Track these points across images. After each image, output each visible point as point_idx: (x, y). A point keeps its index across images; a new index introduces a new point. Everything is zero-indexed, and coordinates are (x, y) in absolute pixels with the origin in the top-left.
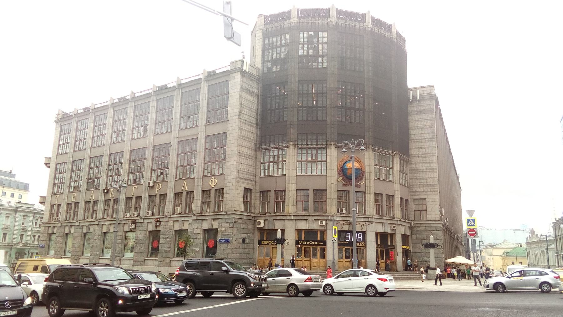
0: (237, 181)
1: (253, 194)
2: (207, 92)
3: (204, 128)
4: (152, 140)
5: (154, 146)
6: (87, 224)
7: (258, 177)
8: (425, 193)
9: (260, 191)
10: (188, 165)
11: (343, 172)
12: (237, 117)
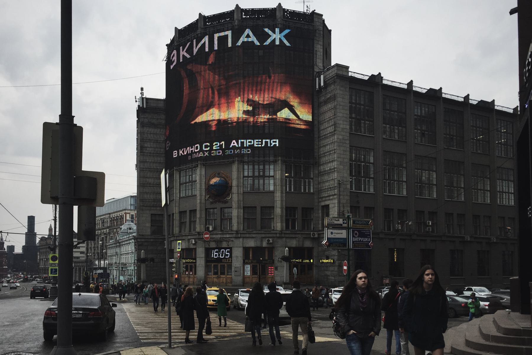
11: (209, 189)
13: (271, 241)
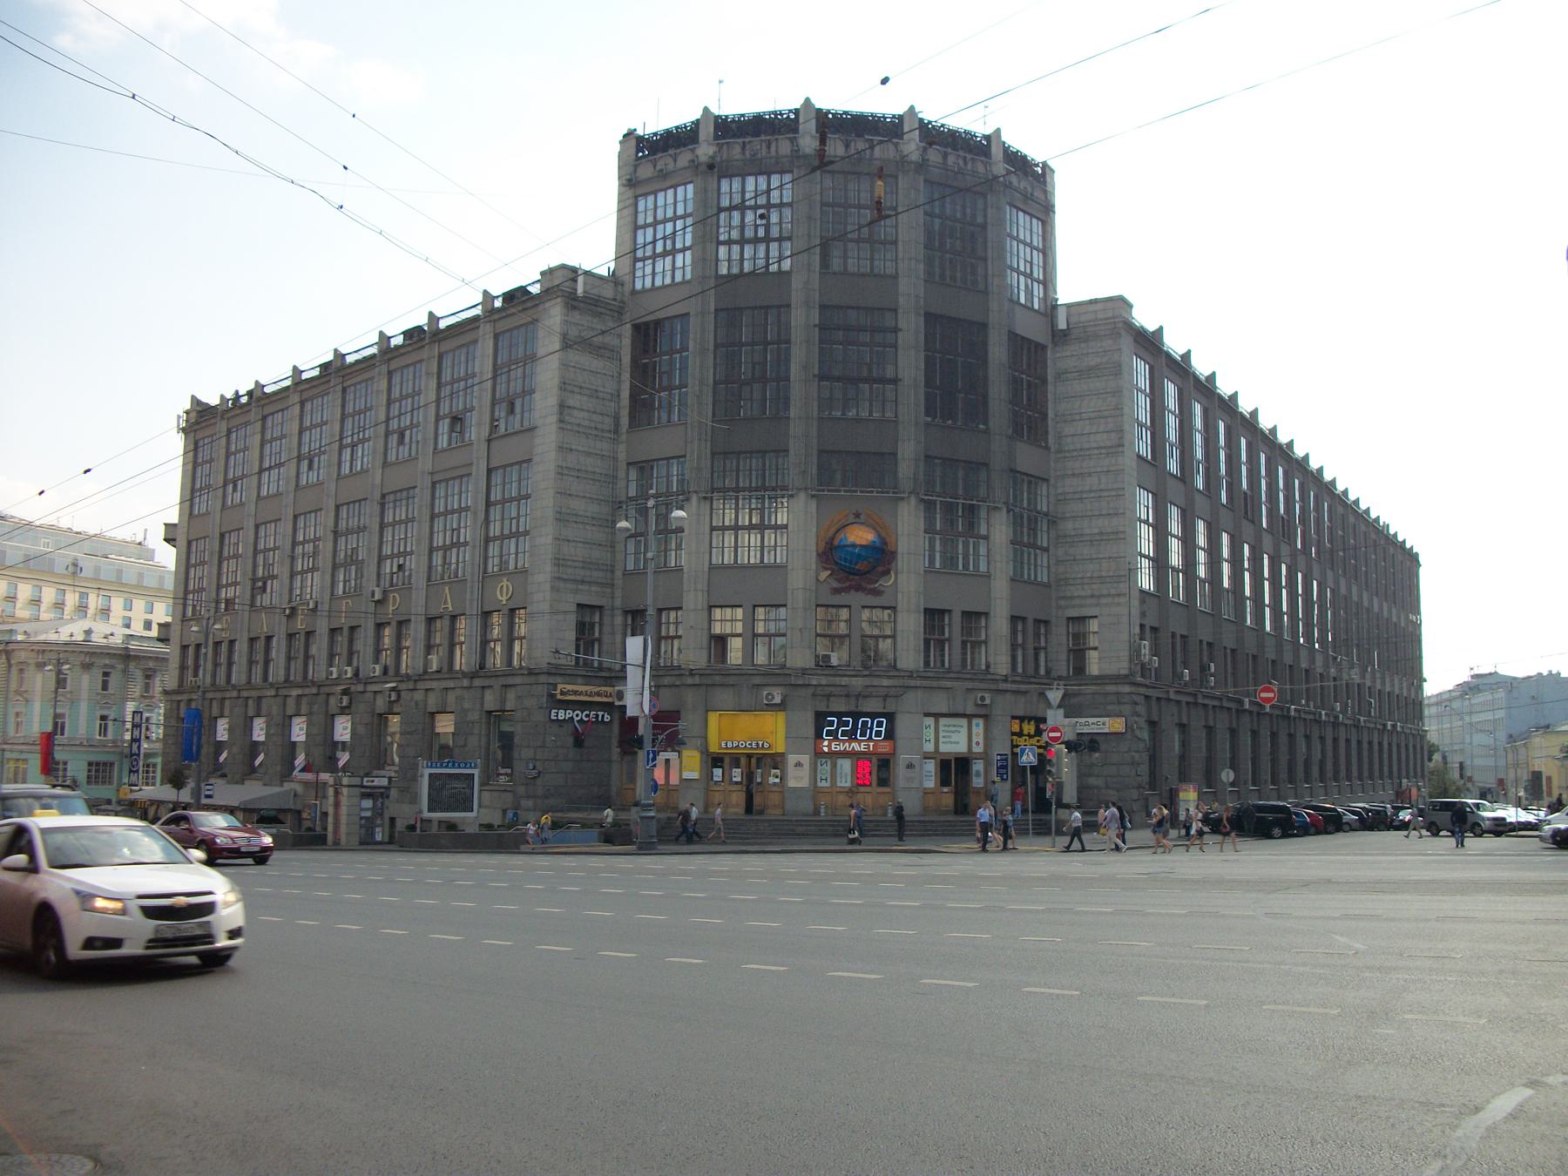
0: (554, 589)
1: (606, 619)
2: (491, 351)
3: (484, 446)
4: (378, 480)
5: (383, 496)
6: (254, 694)
7: (619, 574)
8: (1093, 601)
9: (626, 612)
10: (453, 545)
12: (554, 418)
13: (987, 701)
